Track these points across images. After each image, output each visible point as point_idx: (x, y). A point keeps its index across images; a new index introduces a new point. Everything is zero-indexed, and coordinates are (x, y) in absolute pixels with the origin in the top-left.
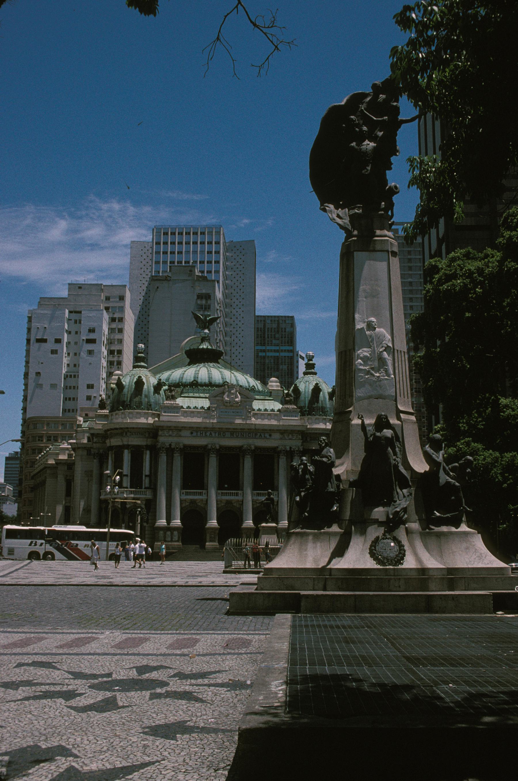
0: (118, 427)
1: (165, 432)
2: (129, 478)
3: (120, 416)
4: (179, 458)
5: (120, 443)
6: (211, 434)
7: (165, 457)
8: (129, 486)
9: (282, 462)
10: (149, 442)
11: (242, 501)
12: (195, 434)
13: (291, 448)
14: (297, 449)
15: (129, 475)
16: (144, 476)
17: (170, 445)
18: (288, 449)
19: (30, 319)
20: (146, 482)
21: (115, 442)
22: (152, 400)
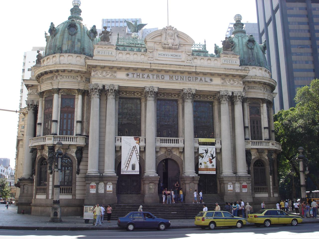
0: (47, 70)
1: (99, 74)
2: (59, 124)
3: (51, 61)
4: (114, 100)
5: (50, 88)
6: (148, 76)
7: (98, 100)
8: (58, 133)
9: (225, 107)
10: (82, 87)
11: (184, 149)
12: (131, 76)
13: (233, 93)
14: (239, 94)
15: (59, 121)
16: (75, 122)
17: (104, 86)
18: (231, 94)
19: (25, 57)
20: (77, 129)
21: (45, 87)
22: (86, 46)
